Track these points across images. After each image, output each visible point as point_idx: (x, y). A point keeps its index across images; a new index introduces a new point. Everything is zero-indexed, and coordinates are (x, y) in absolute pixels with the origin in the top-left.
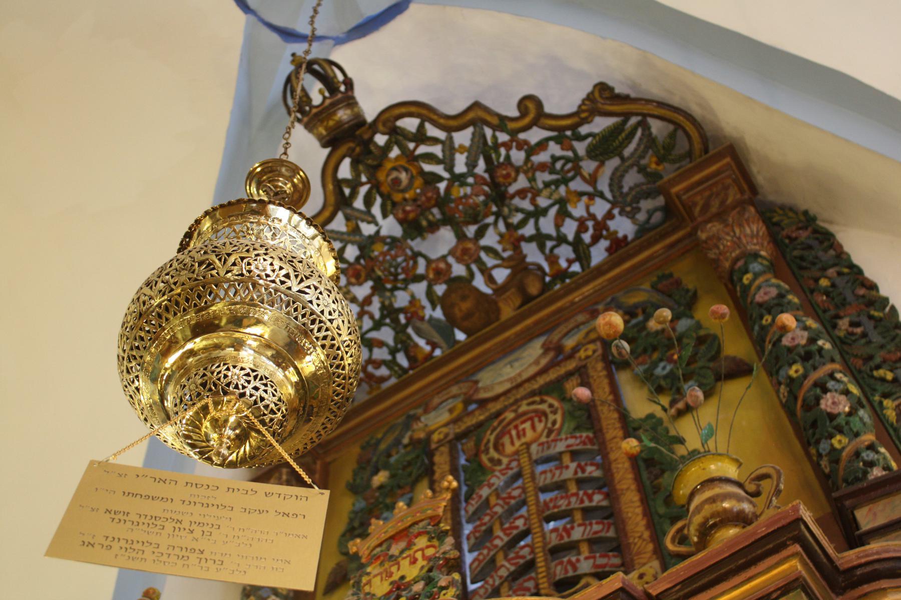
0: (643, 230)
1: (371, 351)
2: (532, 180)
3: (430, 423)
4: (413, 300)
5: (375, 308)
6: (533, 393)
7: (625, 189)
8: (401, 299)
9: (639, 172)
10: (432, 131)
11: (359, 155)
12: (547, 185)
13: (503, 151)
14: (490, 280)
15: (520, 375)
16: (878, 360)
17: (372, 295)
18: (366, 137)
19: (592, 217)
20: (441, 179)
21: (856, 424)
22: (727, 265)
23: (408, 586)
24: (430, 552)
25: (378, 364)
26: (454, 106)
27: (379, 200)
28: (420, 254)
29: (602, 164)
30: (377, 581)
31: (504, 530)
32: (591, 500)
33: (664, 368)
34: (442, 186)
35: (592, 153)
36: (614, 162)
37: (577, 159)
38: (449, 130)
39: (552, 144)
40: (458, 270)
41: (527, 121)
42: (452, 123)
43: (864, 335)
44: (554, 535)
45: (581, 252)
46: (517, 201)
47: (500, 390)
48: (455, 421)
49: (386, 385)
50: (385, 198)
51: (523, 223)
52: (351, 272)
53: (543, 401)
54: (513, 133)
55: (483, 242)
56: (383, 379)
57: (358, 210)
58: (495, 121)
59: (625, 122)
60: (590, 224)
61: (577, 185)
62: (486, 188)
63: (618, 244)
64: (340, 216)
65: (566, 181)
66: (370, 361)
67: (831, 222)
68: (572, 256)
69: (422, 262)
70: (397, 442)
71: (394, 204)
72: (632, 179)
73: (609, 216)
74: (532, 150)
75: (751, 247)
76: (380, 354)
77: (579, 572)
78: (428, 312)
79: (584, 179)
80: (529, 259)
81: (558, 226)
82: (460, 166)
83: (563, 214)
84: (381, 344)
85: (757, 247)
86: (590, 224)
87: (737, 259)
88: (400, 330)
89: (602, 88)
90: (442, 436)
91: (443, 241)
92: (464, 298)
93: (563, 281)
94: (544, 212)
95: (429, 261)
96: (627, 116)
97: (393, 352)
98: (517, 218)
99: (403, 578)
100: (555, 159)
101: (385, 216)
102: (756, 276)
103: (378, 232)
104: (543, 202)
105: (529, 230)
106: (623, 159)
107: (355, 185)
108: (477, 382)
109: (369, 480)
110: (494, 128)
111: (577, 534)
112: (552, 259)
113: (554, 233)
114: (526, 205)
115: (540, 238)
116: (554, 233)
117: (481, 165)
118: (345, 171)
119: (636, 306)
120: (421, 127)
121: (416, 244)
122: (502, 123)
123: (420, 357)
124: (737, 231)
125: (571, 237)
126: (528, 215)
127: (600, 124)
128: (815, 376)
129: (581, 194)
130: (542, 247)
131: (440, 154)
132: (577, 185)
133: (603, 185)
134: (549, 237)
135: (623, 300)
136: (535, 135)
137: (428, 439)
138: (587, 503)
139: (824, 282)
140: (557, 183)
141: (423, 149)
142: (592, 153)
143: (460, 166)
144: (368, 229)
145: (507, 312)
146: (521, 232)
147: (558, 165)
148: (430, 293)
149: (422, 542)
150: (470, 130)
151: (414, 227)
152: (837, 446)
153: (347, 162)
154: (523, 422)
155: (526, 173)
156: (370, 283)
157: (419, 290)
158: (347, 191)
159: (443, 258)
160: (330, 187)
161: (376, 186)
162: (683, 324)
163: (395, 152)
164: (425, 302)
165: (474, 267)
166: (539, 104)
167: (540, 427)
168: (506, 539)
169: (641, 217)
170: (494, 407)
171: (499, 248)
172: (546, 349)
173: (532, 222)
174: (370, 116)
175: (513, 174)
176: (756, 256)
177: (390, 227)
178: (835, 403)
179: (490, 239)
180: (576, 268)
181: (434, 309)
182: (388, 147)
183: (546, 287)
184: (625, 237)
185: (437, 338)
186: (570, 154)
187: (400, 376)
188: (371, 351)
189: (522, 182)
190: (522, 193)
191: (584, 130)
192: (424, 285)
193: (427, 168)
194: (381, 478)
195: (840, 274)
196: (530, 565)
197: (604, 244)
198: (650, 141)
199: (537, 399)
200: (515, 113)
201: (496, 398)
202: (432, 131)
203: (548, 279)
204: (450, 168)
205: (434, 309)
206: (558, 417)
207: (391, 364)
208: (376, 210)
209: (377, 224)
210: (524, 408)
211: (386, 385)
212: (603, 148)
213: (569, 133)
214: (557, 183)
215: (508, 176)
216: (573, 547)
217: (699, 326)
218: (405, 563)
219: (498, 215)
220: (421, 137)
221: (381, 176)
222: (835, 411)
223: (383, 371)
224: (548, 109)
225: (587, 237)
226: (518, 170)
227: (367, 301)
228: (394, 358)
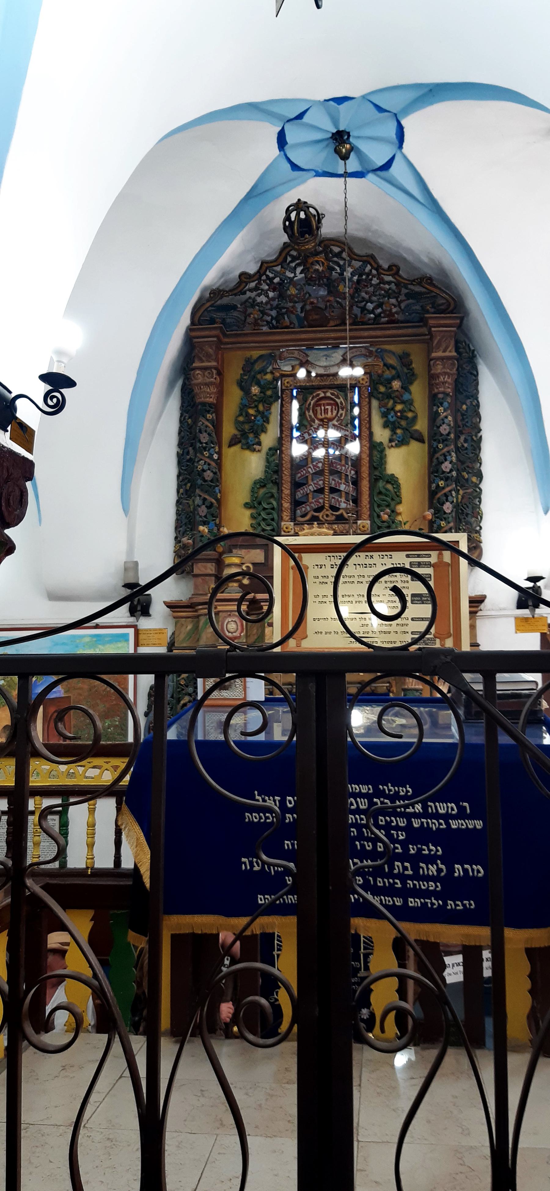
22: (436, 390)
29: (408, 299)
38: (352, 259)
43: (466, 449)
64: (280, 266)
67: (480, 356)
74: (382, 281)
97: (272, 318)
110: (372, 267)
122: (378, 268)
135: (386, 358)
142: (406, 295)
158: (289, 259)
168: (314, 471)
189: (371, 289)
191: (409, 286)
205: (301, 312)
210: (328, 394)
227: (273, 299)
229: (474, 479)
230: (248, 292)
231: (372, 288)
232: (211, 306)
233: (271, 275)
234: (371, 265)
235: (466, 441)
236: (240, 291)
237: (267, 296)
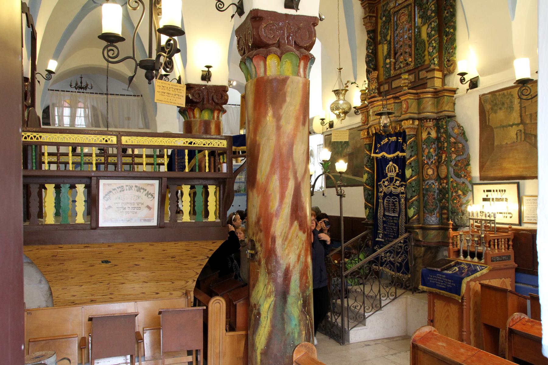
16: (447, 25)
48: (394, 7)
229: (452, 30)
235: (447, 13)
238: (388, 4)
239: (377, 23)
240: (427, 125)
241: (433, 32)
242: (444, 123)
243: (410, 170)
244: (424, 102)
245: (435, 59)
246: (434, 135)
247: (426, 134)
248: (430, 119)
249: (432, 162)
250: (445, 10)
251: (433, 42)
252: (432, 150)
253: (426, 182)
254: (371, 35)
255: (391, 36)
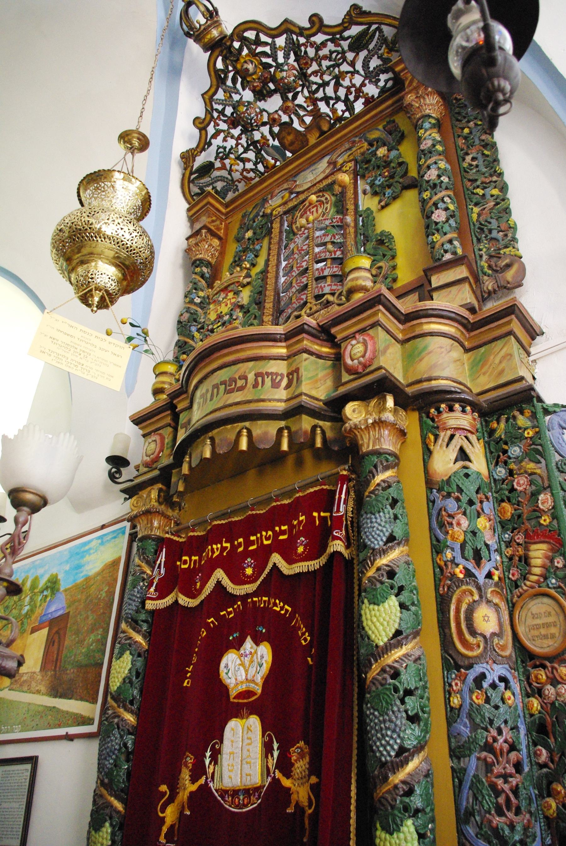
0: (383, 91)
1: (244, 164)
2: (320, 65)
3: (273, 204)
4: (263, 137)
5: (243, 141)
6: (320, 191)
7: (371, 69)
8: (257, 136)
9: (378, 58)
10: (263, 38)
11: (226, 55)
12: (328, 68)
13: (303, 48)
14: (302, 121)
15: (315, 179)
16: (478, 183)
17: (241, 134)
18: (228, 44)
19: (354, 86)
20: (271, 66)
21: (446, 228)
23: (223, 316)
24: (233, 300)
25: (248, 171)
26: (273, 23)
27: (240, 80)
28: (264, 110)
29: (358, 54)
30: (212, 313)
31: (297, 267)
32: (335, 255)
33: (379, 180)
34: (272, 70)
35: (352, 48)
36: (363, 54)
37: (344, 52)
38: (273, 37)
39: (329, 43)
40: (285, 118)
41: (314, 30)
42: (274, 33)
43: (477, 166)
44: (317, 272)
45: (350, 107)
46: (313, 78)
47: (305, 187)
48: (285, 203)
49: (253, 182)
50: (243, 79)
51: (317, 90)
52: (229, 121)
53: (323, 196)
54: (308, 37)
55: (296, 102)
56: (252, 179)
57: (229, 87)
58: (297, 30)
59: (368, 29)
60: (353, 89)
61: (345, 67)
62: (295, 72)
63: (369, 101)
64: (220, 91)
65: (338, 65)
66: (244, 169)
68: (344, 108)
69: (265, 115)
70: (257, 215)
71: (248, 82)
72: (374, 63)
73: (363, 85)
74: (318, 48)
75: (427, 112)
76: (250, 165)
77: (324, 292)
78: (271, 142)
79: (348, 63)
80: (322, 111)
81: (336, 91)
82: (281, 60)
83: (338, 85)
84: (249, 160)
85: (431, 112)
86: (353, 89)
87: (419, 119)
88: (258, 153)
89: (355, 7)
90: (277, 213)
91: (274, 103)
92: (289, 134)
93: (341, 123)
94: (327, 84)
95: (269, 114)
96: (370, 24)
97: (256, 164)
98: (314, 87)
99: (221, 312)
100: (331, 52)
101: (244, 89)
102: (426, 130)
103: (241, 98)
104: (327, 78)
105: (320, 94)
106: (368, 50)
107: (226, 71)
108: (295, 181)
109: (244, 235)
111: (326, 273)
112: (334, 111)
113: (334, 96)
114: (317, 80)
115: (326, 99)
116: (334, 96)
117: (292, 56)
118: (220, 65)
119: (375, 140)
120: (257, 36)
121: (261, 104)
122: (301, 31)
123: (270, 166)
124: (422, 100)
125: (343, 98)
126: (320, 86)
127: (355, 30)
128: (435, 198)
129: (347, 72)
130: (328, 104)
131: (269, 52)
132: (345, 67)
133: (359, 66)
134: (331, 98)
136: (319, 38)
137: (271, 214)
138: (333, 256)
139: (466, 131)
140: (334, 66)
141: (259, 49)
142: (352, 48)
143: (281, 60)
144: (236, 97)
145: (312, 140)
146: (316, 96)
147: (334, 55)
148: (271, 132)
149: (231, 295)
150: (285, 36)
151: (261, 94)
152: (435, 240)
153: (220, 58)
154: (313, 208)
155: (316, 61)
156: (240, 128)
157: (265, 130)
158: (223, 76)
159: (276, 111)
160: (213, 73)
161: (237, 72)
162: (394, 153)
163: (245, 51)
164: (269, 137)
165: (293, 116)
166: (321, 20)
167: (320, 211)
168: (297, 272)
169: (382, 84)
170: (302, 197)
171: (305, 105)
172: (329, 163)
173: (321, 89)
174: (229, 31)
175: (309, 62)
176: (429, 116)
177: (248, 95)
178: (439, 216)
179: (300, 100)
180: (347, 114)
181: (274, 140)
182: (241, 49)
183: (332, 126)
184: (373, 96)
185: (277, 157)
186: (339, 49)
187: (260, 177)
188: (244, 164)
189: (314, 67)
190: (315, 73)
191: (346, 34)
192: (268, 126)
193: (264, 60)
194: (249, 234)
195: (476, 125)
196: (306, 286)
197: (361, 100)
198: (383, 40)
199: (321, 194)
200: (308, 25)
201: (303, 192)
202: (263, 38)
203: (332, 121)
204: (275, 60)
205: (274, 140)
206: (329, 205)
207: (255, 170)
208: (239, 86)
209: (240, 94)
211: (253, 182)
212: (358, 44)
213: (338, 36)
214: (334, 66)
215: (306, 63)
216: (324, 277)
217: (400, 156)
218: (223, 305)
219: (303, 86)
220: (258, 42)
221: (239, 66)
222: (438, 221)
223: (252, 175)
224: (326, 22)
225: (351, 97)
226: (312, 60)
227: (239, 138)
228: (256, 167)
229: (495, 192)
230: (213, 141)
231: (314, 63)
232: (191, 173)
233: (220, 107)
234: (295, 33)
236: (206, 143)
237: (232, 137)
238: (265, 201)
239: (222, 253)
240: (452, 423)
241: (445, 179)
242: (522, 421)
243: (393, 602)
244: (431, 348)
245: (456, 243)
246: (479, 463)
247: (453, 456)
248: (464, 403)
249: (489, 575)
250: (467, 154)
251: (447, 199)
252: (482, 523)
253: (472, 674)
254: (205, 270)
255: (267, 261)
